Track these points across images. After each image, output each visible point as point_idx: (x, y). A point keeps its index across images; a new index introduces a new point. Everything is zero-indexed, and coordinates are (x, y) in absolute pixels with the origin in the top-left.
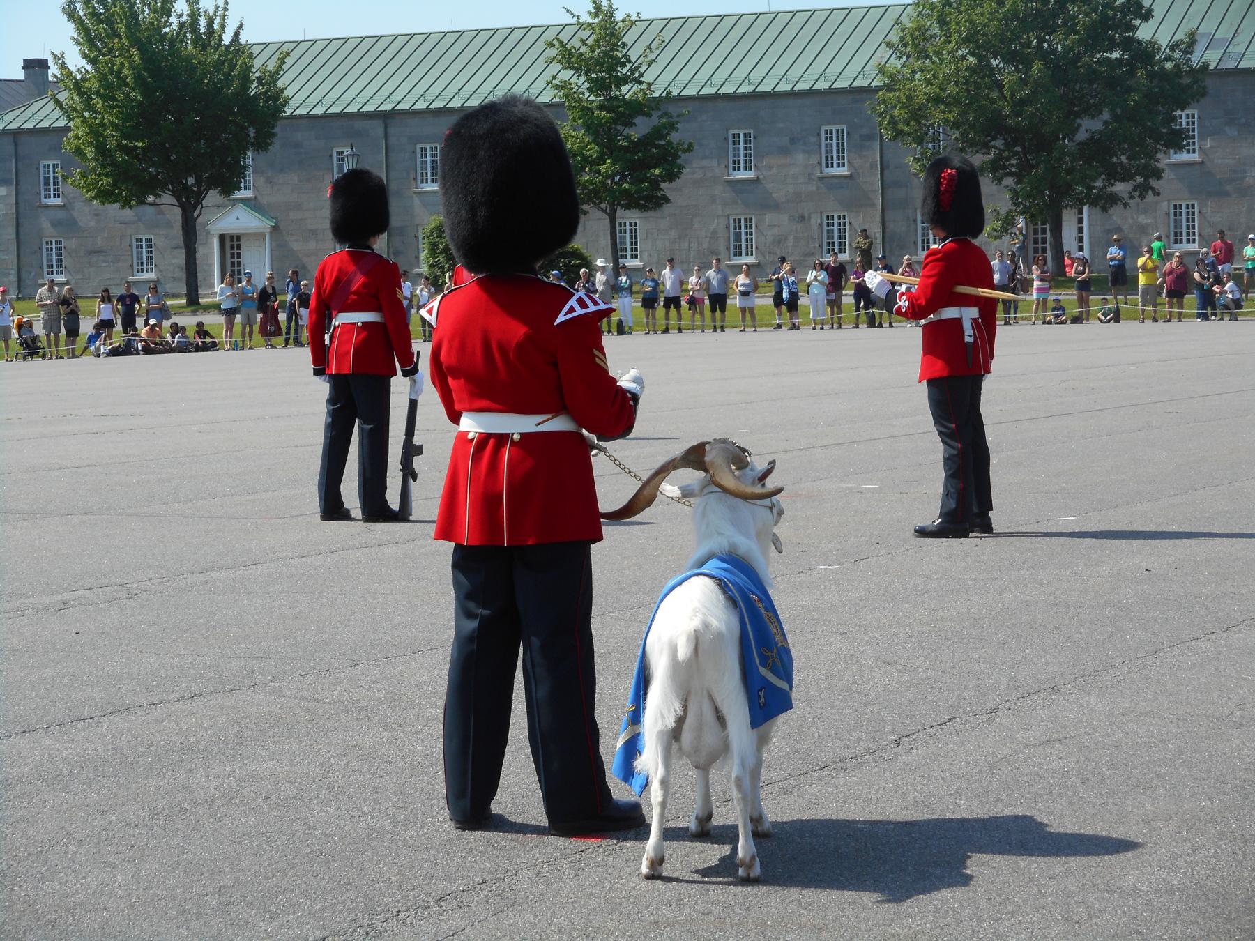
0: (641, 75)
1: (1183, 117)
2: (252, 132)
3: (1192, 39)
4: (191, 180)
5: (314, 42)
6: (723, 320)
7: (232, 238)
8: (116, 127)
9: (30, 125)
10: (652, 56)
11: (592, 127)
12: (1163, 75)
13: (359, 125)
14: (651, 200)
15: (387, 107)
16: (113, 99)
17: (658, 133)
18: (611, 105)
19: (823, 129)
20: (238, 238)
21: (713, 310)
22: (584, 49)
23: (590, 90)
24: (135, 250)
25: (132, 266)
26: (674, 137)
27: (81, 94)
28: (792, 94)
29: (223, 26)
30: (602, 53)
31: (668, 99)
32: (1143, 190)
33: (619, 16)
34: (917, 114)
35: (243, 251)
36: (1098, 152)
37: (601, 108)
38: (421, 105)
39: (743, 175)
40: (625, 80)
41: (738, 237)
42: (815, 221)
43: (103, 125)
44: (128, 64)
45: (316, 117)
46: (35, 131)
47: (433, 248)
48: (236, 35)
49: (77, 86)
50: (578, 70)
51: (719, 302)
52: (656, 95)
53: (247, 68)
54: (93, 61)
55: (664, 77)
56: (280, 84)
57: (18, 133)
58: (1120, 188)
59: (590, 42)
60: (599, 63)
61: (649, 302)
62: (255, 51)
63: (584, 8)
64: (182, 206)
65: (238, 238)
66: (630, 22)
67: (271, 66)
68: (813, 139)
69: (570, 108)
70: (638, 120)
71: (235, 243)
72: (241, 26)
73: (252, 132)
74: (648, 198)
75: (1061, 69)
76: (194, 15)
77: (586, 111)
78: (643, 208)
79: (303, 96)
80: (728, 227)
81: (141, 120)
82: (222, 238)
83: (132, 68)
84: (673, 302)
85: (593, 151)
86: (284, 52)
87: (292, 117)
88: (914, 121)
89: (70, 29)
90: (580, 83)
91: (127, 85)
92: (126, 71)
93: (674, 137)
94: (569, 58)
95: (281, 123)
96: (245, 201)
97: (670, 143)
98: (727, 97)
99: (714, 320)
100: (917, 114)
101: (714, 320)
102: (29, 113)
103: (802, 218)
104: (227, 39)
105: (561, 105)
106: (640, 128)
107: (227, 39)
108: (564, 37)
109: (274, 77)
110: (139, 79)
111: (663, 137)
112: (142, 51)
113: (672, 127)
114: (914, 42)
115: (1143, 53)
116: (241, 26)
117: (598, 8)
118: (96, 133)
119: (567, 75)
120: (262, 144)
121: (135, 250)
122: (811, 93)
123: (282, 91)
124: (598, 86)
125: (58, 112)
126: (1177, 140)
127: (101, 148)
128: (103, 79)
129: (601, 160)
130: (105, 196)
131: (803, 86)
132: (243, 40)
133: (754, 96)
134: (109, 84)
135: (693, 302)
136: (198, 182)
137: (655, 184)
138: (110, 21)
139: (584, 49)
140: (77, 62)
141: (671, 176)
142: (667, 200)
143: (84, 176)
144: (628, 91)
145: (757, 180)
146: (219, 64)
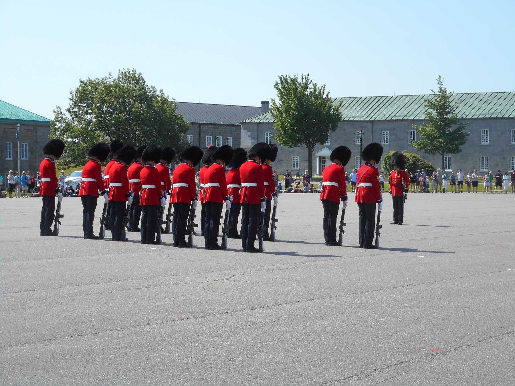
0: (454, 111)
2: (331, 125)
4: (311, 140)
6: (477, 189)
7: (323, 158)
8: (289, 122)
9: (262, 121)
10: (457, 105)
11: (438, 127)
13: (364, 124)
14: (455, 150)
15: (373, 119)
16: (289, 114)
17: (458, 130)
18: (444, 120)
19: (512, 130)
20: (325, 158)
21: (474, 186)
22: (436, 103)
23: (437, 116)
24: (511, 162)
26: (464, 131)
27: (279, 112)
28: (502, 118)
29: (323, 93)
30: (442, 103)
31: (462, 119)
33: (448, 92)
35: (326, 162)
37: (441, 121)
38: (384, 119)
39: (485, 143)
40: (449, 113)
41: (483, 163)
43: (285, 122)
44: (293, 103)
45: (351, 121)
46: (264, 123)
47: (386, 163)
48: (327, 95)
50: (434, 109)
51: (475, 184)
52: (458, 117)
53: (330, 106)
54: (283, 102)
55: (460, 112)
56: (340, 111)
57: (259, 123)
59: (438, 100)
60: (440, 107)
61: (453, 183)
62: (333, 100)
63: (437, 90)
64: (308, 147)
66: (451, 94)
67: (338, 105)
68: (508, 133)
69: (431, 121)
70: (452, 125)
72: (329, 93)
73: (331, 125)
74: (454, 150)
76: (315, 89)
77: (436, 122)
78: (452, 153)
80: (480, 160)
81: (297, 121)
82: (320, 158)
83: (295, 104)
84: (460, 183)
85: (437, 135)
86: (342, 101)
87: (343, 121)
89: (276, 92)
90: (435, 113)
91: (293, 109)
92: (292, 105)
93: (464, 131)
94: (431, 105)
95: (339, 123)
96: (327, 147)
97: (462, 133)
98: (481, 119)
99: (474, 189)
101: (474, 189)
102: (262, 117)
103: (504, 158)
104: (324, 97)
105: (428, 120)
106: (453, 128)
107: (324, 97)
108: (430, 98)
109: (338, 108)
110: (296, 107)
111: (460, 131)
112: (298, 99)
113: (463, 128)
116: (329, 93)
117: (441, 89)
118: (283, 124)
119: (430, 110)
120: (333, 129)
121: (511, 162)
122: (509, 118)
123: (340, 113)
124: (440, 114)
125: (272, 117)
127: (284, 129)
128: (286, 107)
129: (440, 138)
130: (285, 143)
131: (506, 116)
132: (329, 97)
133: (490, 119)
134: (287, 110)
135: (468, 184)
136: (313, 140)
137: (457, 146)
138: (289, 90)
140: (278, 102)
141: (462, 144)
142: (461, 151)
143: (279, 137)
144: (449, 116)
145: (490, 146)
146: (322, 104)
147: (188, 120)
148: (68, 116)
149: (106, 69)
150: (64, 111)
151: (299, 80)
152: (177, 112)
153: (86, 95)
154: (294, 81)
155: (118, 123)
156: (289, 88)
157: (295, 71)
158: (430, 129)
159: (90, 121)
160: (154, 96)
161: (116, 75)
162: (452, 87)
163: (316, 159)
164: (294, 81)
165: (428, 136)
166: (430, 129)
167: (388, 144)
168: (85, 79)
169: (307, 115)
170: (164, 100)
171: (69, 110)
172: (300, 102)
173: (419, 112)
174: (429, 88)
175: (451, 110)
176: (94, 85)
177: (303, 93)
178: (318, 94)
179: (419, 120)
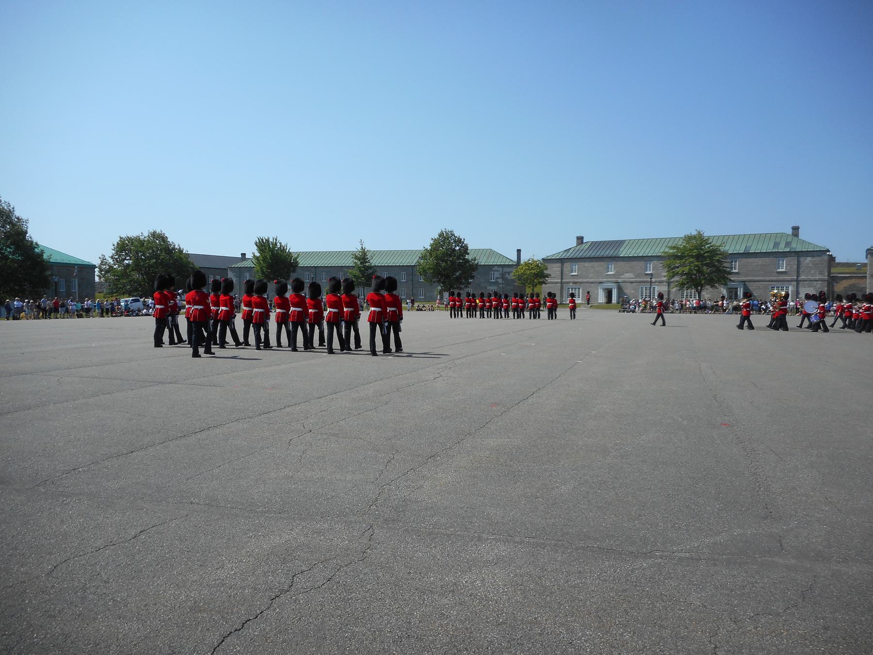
1: (474, 274)
3: (475, 260)
11: (360, 271)
12: (470, 265)
18: (364, 267)
30: (363, 257)
32: (466, 287)
34: (425, 271)
36: (458, 279)
44: (268, 255)
49: (257, 258)
55: (375, 262)
58: (462, 286)
63: (359, 248)
75: (453, 262)
77: (360, 268)
79: (302, 263)
81: (270, 266)
88: (424, 272)
94: (356, 258)
100: (425, 271)
106: (370, 271)
114: (423, 257)
115: (468, 261)
118: (261, 268)
120: (294, 271)
126: (472, 277)
127: (262, 271)
134: (264, 259)
140: (258, 254)
147: (198, 265)
148: (111, 261)
149: (140, 229)
150: (107, 258)
151: (271, 240)
152: (189, 260)
153: (124, 247)
154: (268, 241)
155: (150, 266)
156: (263, 245)
157: (269, 234)
158: (357, 273)
159: (128, 265)
160: (174, 249)
161: (146, 234)
162: (368, 247)
164: (268, 241)
165: (355, 276)
166: (357, 273)
168: (124, 236)
169: (276, 261)
170: (181, 251)
171: (112, 257)
172: (273, 254)
173: (350, 262)
174: (355, 247)
176: (130, 239)
177: (273, 248)
178: (283, 250)
179: (348, 267)
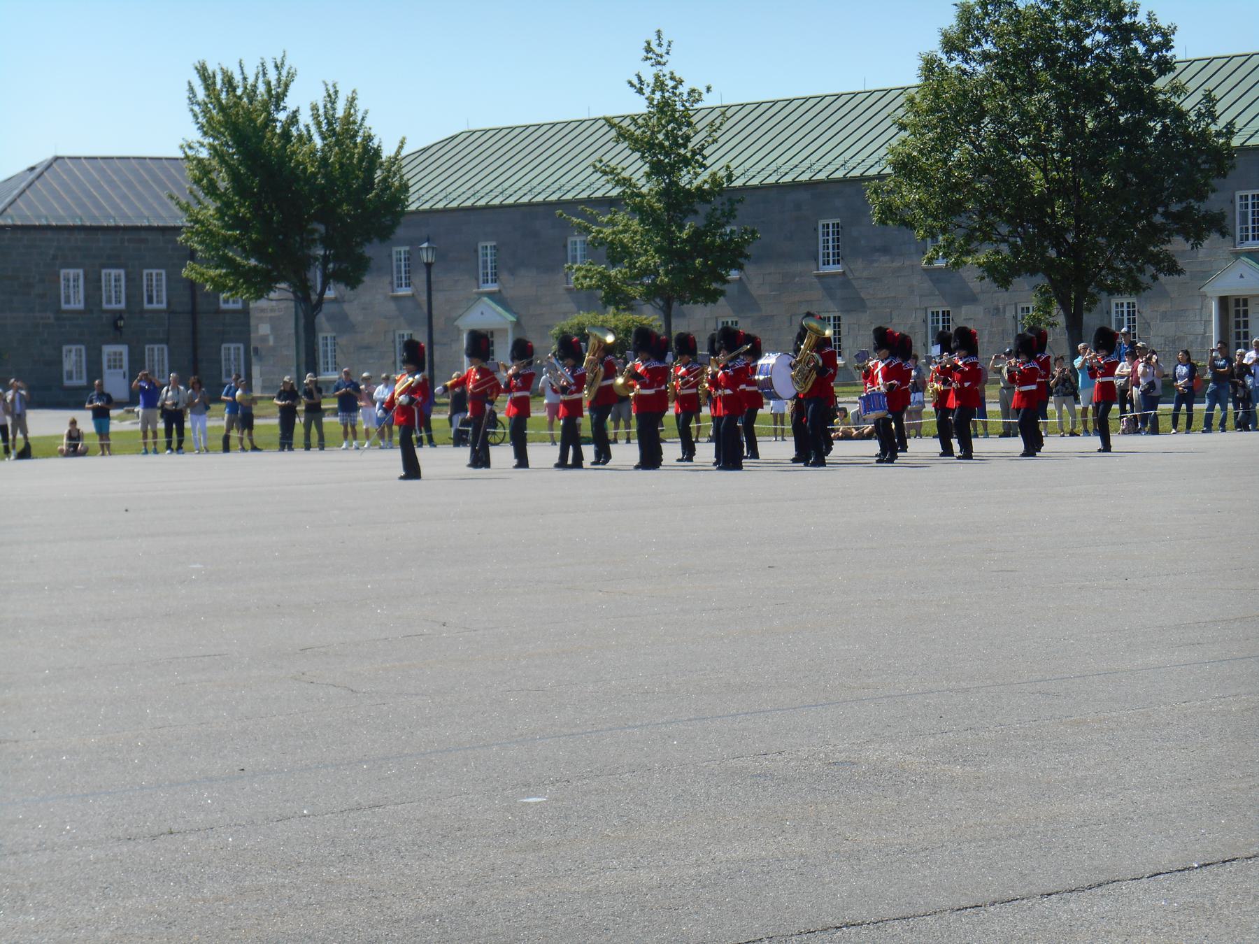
0: (705, 158)
5: (596, 120)
7: (1237, 301)
17: (714, 224)
20: (1245, 302)
25: (395, 363)
30: (666, 131)
42: (1009, 314)
45: (494, 207)
65: (1245, 302)
71: (1241, 309)
72: (366, 112)
80: (925, 321)
82: (1223, 301)
90: (636, 169)
96: (490, 295)
103: (997, 309)
116: (366, 112)
124: (657, 169)
139: (632, 128)
163: (1204, 307)
167: (837, 269)
175: (694, 153)
